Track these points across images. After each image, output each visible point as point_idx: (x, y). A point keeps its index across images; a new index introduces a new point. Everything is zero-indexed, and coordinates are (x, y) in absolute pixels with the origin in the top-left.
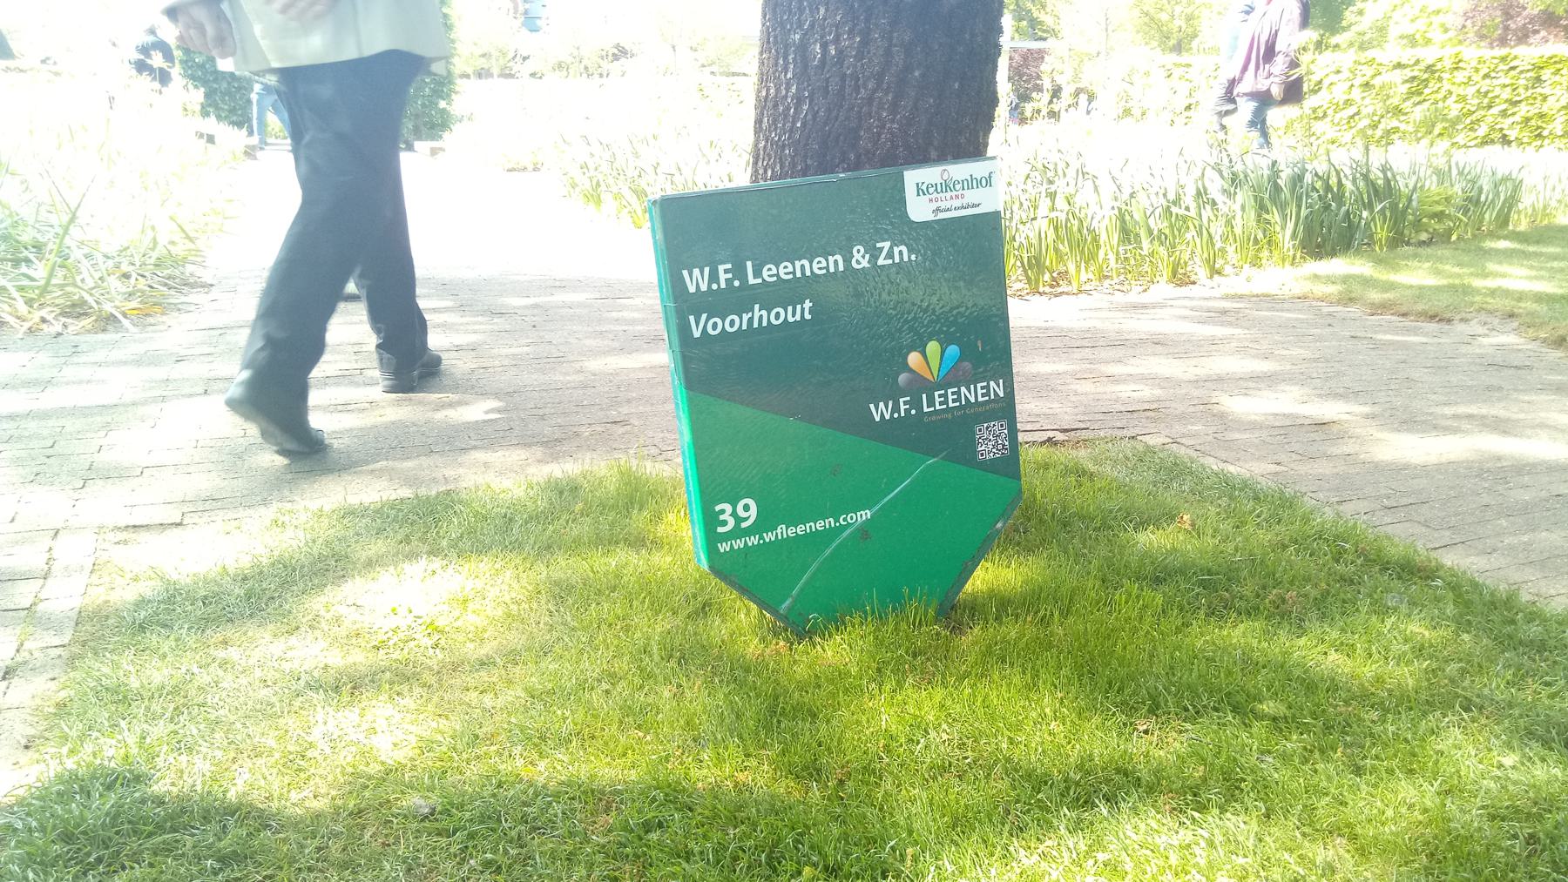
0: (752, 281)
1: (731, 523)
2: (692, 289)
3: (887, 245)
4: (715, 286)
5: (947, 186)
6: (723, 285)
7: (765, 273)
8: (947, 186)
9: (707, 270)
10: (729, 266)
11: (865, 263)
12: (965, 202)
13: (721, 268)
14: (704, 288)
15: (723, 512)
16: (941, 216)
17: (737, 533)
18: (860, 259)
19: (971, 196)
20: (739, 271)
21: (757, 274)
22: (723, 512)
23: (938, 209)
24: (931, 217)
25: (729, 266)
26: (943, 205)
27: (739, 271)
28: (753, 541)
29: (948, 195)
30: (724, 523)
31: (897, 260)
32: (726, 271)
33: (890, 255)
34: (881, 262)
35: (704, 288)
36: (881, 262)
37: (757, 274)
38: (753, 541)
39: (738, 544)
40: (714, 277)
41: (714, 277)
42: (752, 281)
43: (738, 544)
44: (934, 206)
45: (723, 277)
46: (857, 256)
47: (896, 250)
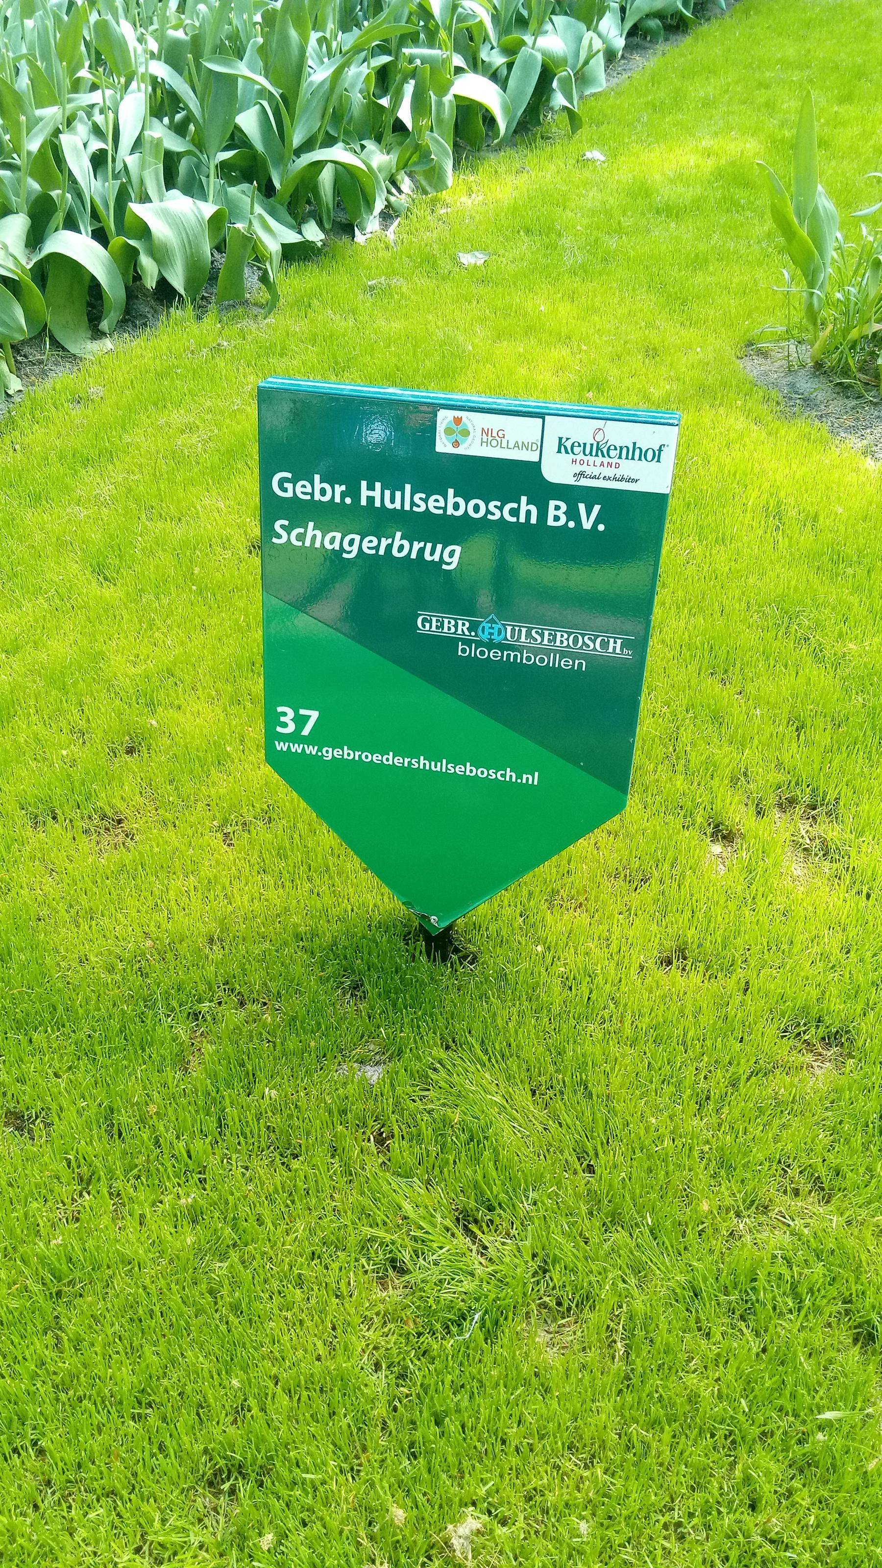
1: (291, 728)
5: (598, 449)
8: (598, 449)
12: (619, 473)
15: (284, 714)
16: (584, 482)
17: (296, 737)
19: (628, 468)
22: (284, 714)
23: (582, 474)
24: (571, 481)
26: (589, 470)
28: (311, 750)
29: (600, 459)
30: (285, 725)
38: (311, 750)
39: (296, 748)
43: (296, 748)
44: (578, 468)
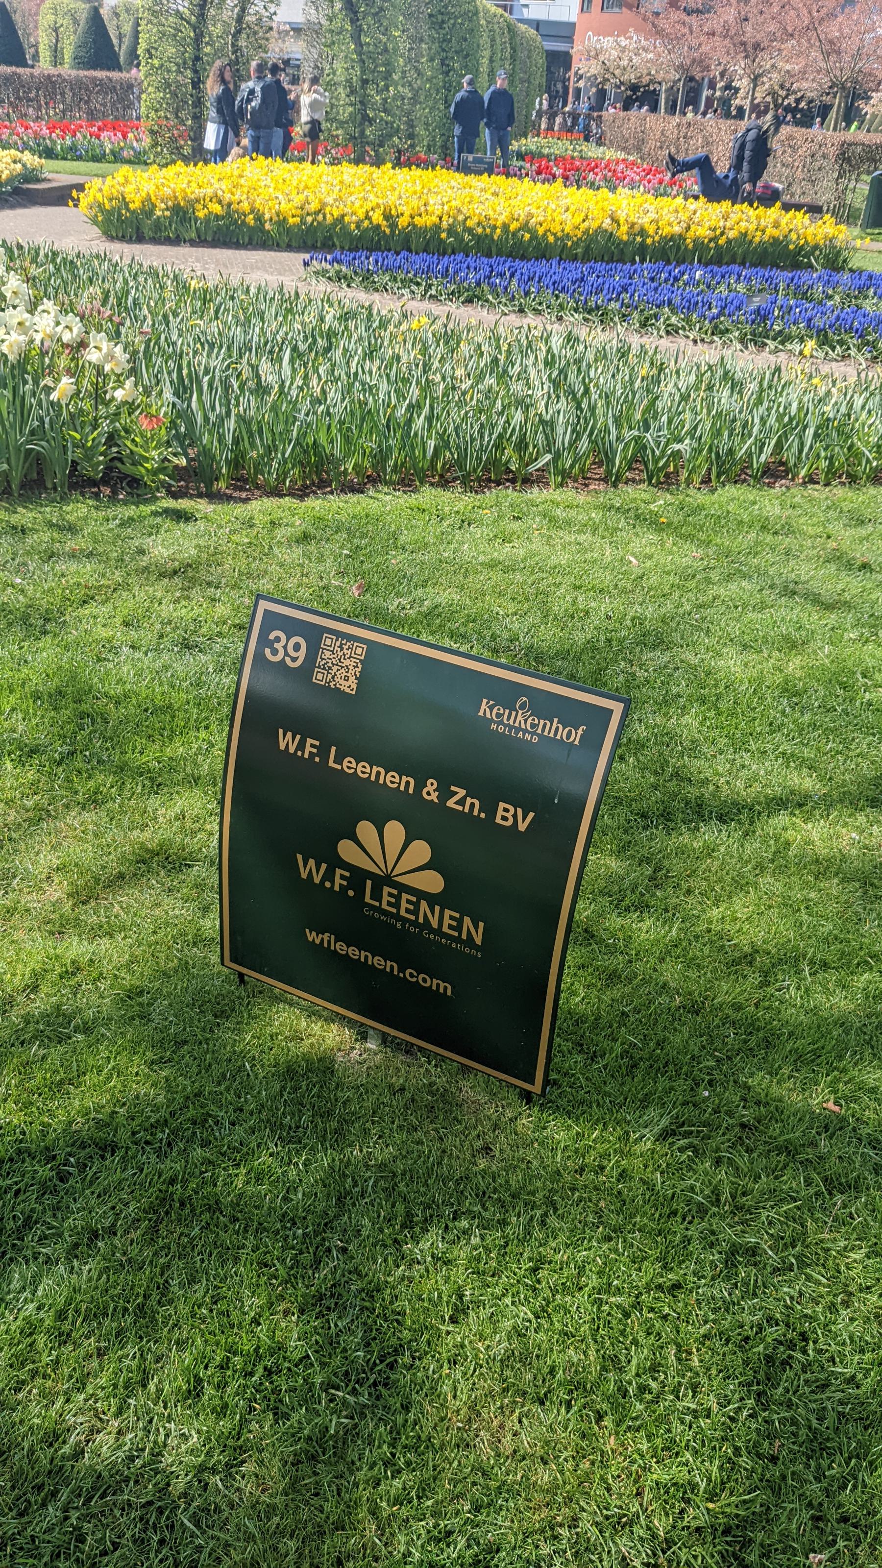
0: (331, 763)
2: (282, 747)
3: (462, 792)
4: (299, 753)
6: (306, 756)
7: (345, 763)
9: (298, 737)
10: (317, 743)
11: (434, 797)
13: (309, 741)
14: (292, 750)
18: (431, 791)
20: (323, 751)
21: (339, 760)
25: (317, 743)
27: (323, 751)
31: (467, 810)
32: (312, 746)
33: (461, 802)
34: (451, 803)
35: (292, 750)
36: (451, 803)
37: (339, 760)
40: (301, 746)
41: (301, 746)
42: (331, 763)
45: (308, 749)
46: (429, 788)
47: (469, 800)
